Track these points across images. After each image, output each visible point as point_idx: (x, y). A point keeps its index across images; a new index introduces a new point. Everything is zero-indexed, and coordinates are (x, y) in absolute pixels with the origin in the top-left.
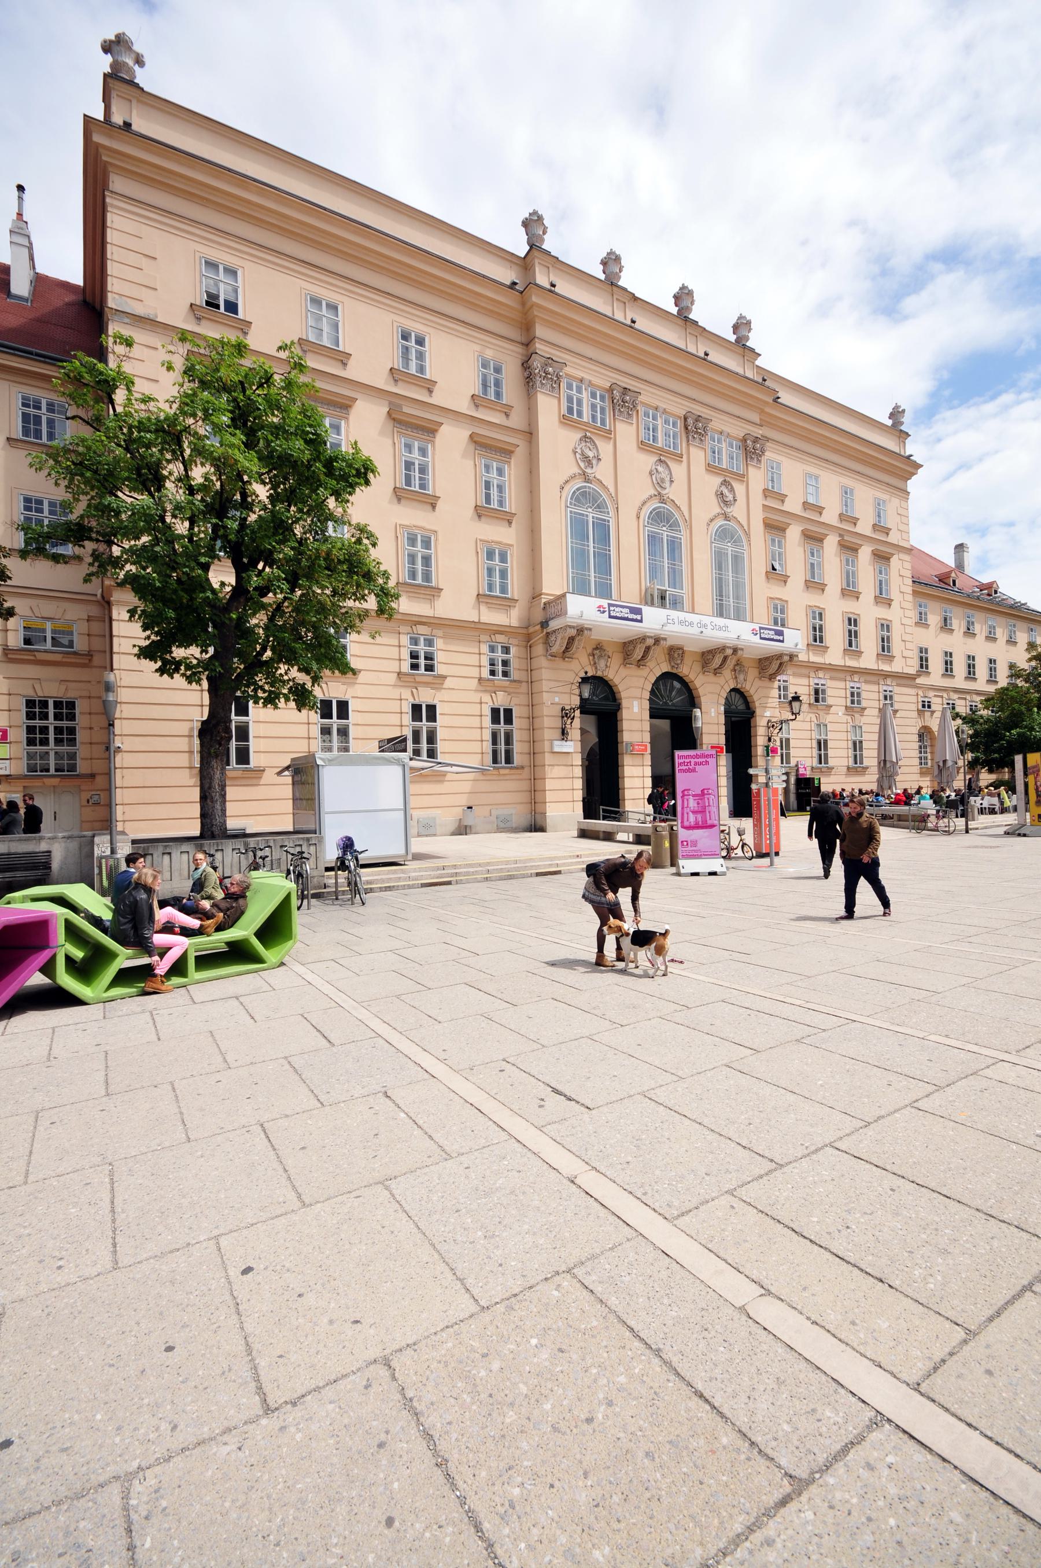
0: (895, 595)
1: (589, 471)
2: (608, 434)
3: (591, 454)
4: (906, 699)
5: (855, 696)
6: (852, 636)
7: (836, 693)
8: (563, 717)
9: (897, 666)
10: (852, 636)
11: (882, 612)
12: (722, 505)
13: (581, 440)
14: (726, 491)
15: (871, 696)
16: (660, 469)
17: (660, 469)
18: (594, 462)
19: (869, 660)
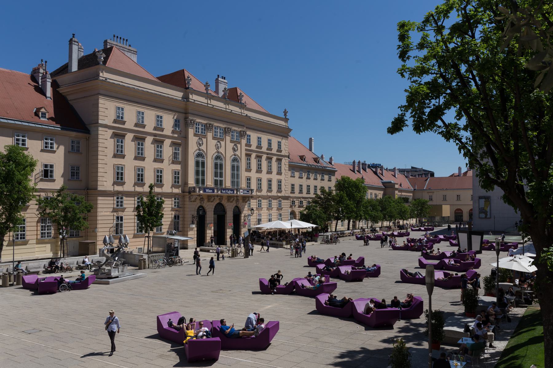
7: (265, 203)
9: (283, 194)
11: (279, 177)
16: (218, 144)
17: (218, 144)
19: (274, 193)
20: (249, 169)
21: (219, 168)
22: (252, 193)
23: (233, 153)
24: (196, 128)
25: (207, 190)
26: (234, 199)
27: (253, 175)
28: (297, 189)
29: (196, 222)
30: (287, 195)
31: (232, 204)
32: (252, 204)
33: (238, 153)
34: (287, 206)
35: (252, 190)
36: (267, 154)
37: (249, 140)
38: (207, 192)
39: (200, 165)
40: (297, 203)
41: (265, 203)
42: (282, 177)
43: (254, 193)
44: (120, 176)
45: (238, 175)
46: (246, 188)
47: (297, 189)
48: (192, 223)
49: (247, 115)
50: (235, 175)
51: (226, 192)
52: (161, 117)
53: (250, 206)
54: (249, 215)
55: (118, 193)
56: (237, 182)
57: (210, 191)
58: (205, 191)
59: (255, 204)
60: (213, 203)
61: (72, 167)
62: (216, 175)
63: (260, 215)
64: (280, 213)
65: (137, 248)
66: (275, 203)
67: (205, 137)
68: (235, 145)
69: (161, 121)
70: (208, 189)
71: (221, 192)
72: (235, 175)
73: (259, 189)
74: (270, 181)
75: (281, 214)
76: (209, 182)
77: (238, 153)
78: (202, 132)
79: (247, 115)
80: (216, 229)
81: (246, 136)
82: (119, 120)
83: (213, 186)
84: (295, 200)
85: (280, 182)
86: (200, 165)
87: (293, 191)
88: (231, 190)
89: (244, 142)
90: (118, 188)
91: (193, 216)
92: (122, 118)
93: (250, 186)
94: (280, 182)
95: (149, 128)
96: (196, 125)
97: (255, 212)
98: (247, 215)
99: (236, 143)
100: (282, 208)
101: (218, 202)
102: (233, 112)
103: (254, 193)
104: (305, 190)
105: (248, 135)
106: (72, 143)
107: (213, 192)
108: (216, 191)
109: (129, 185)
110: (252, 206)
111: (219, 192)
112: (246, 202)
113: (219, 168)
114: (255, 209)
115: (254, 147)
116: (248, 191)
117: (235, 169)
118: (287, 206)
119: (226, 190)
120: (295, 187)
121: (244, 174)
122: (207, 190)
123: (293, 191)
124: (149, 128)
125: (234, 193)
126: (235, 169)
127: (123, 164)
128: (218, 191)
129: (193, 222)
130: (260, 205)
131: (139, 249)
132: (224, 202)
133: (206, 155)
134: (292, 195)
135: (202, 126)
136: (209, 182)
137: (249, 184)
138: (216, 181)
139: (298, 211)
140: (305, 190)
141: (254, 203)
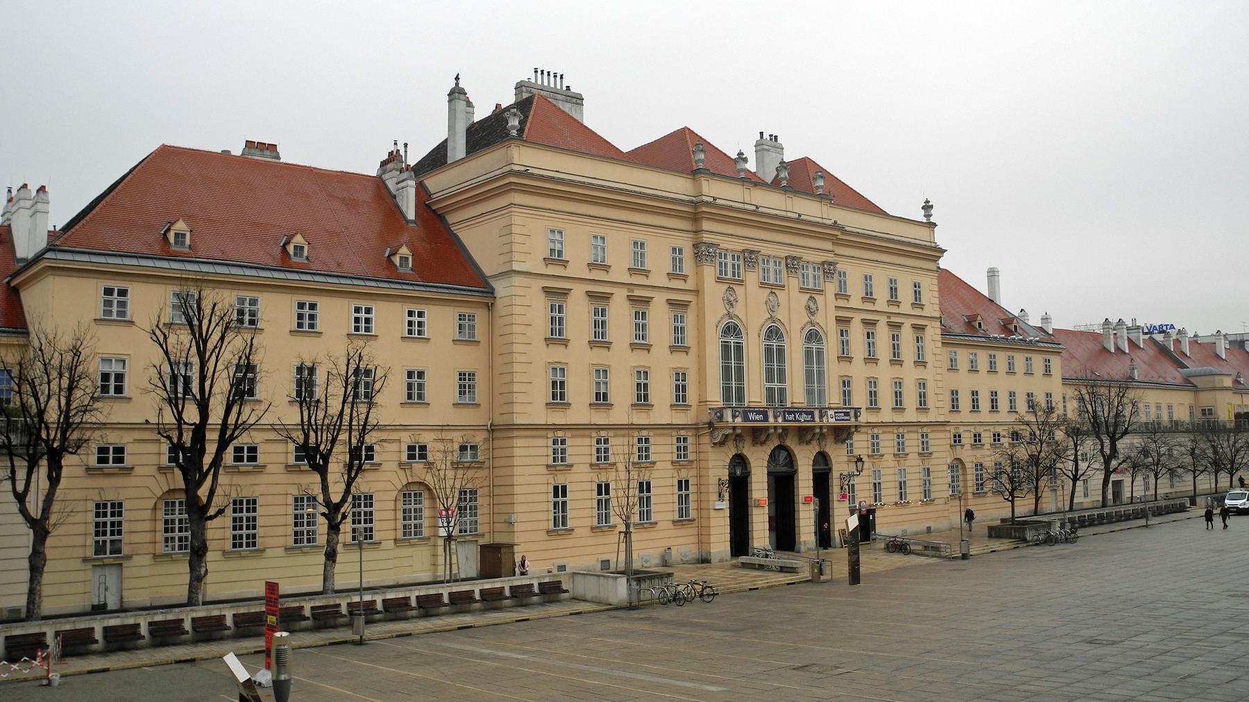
0: (929, 358)
1: (731, 310)
2: (741, 283)
3: (732, 299)
4: (940, 442)
5: (901, 446)
6: (898, 395)
7: (887, 443)
8: (719, 485)
9: (932, 417)
10: (898, 395)
11: (920, 373)
12: (809, 315)
13: (727, 290)
14: (812, 305)
15: (912, 442)
16: (771, 298)
17: (771, 298)
18: (734, 303)
19: (911, 415)
20: (845, 357)
21: (775, 355)
22: (856, 417)
23: (807, 319)
24: (721, 263)
25: (751, 416)
26: (814, 435)
27: (858, 371)
28: (965, 402)
29: (727, 496)
30: (941, 419)
31: (810, 447)
32: (855, 445)
33: (819, 319)
34: (943, 448)
35: (857, 410)
36: (889, 314)
37: (842, 285)
38: (752, 421)
39: (732, 354)
40: (967, 439)
41: (887, 443)
42: (928, 374)
43: (864, 417)
44: (559, 390)
45: (821, 374)
46: (842, 405)
47: (965, 402)
48: (718, 498)
49: (835, 222)
50: (814, 377)
51: (795, 417)
52: (642, 244)
53: (852, 451)
54: (851, 475)
55: (556, 428)
56: (819, 391)
57: (758, 417)
58: (746, 419)
59: (864, 444)
60: (765, 447)
61: (460, 374)
62: (770, 378)
63: (877, 473)
64: (926, 467)
65: (600, 560)
66: (912, 442)
67: (741, 283)
68: (812, 298)
69: (642, 255)
70: (753, 412)
71: (785, 420)
72: (814, 377)
73: (874, 406)
74: (898, 383)
75: (928, 469)
76: (755, 394)
77: (819, 319)
78: (734, 276)
79: (835, 222)
80: (773, 514)
81: (836, 275)
82: (556, 258)
83: (764, 404)
84: (961, 430)
85: (922, 384)
86: (732, 354)
87: (955, 407)
88: (807, 413)
89: (831, 288)
90: (557, 418)
91: (720, 480)
92: (560, 253)
93: (849, 400)
94: (922, 384)
95: (619, 273)
96: (721, 257)
97: (867, 464)
98: (845, 473)
99: (813, 293)
100: (931, 454)
101: (777, 443)
102: (802, 217)
103: (864, 417)
104: (985, 403)
105: (840, 273)
106: (460, 319)
107: (766, 419)
108: (770, 414)
109: (579, 411)
110: (856, 452)
111: (780, 420)
112: (843, 442)
113: (775, 355)
114: (865, 458)
115: (856, 302)
116: (847, 414)
117: (813, 357)
118: (943, 448)
119: (794, 413)
120: (960, 396)
121: (833, 370)
122: (751, 416)
123: (955, 407)
124: (619, 273)
125: (814, 421)
126: (813, 357)
127: (564, 361)
128: (776, 417)
129: (720, 496)
130: (875, 447)
131: (602, 561)
132: (791, 443)
133: (746, 329)
134: (954, 418)
135: (734, 259)
136: (755, 394)
137: (847, 395)
138: (770, 391)
139: (970, 459)
140: (985, 403)
141: (860, 443)
